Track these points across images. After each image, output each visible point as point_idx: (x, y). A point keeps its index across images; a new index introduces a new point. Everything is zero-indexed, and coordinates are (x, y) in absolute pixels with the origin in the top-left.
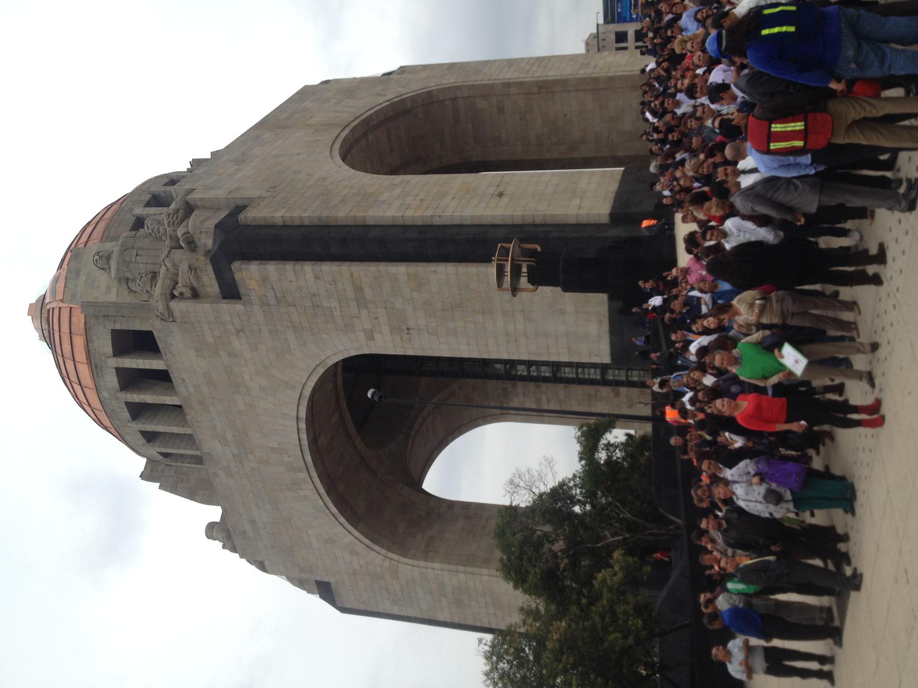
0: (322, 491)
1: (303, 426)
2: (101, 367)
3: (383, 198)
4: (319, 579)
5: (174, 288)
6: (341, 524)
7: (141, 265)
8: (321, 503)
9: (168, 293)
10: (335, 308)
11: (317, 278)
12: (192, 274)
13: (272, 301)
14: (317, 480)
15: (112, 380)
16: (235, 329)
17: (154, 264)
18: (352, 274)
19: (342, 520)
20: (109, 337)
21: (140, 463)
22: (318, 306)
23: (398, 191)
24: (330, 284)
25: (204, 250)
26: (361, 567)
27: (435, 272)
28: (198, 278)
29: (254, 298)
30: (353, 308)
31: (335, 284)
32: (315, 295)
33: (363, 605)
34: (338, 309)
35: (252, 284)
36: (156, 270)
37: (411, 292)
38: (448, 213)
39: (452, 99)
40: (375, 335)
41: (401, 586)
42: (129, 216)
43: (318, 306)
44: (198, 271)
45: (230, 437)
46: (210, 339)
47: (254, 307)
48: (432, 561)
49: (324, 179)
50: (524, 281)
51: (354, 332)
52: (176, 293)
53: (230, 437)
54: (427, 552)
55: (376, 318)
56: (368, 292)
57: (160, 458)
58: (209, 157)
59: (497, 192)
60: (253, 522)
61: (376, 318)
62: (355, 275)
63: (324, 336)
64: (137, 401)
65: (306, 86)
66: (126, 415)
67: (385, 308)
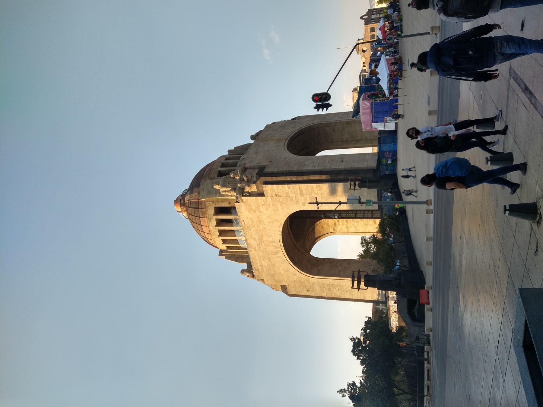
1: (281, 233)
2: (211, 219)
3: (306, 163)
4: (282, 284)
11: (289, 188)
14: (284, 251)
17: (234, 186)
18: (299, 187)
19: (291, 263)
22: (288, 196)
23: (310, 161)
29: (269, 195)
30: (299, 196)
32: (287, 193)
34: (295, 197)
35: (269, 191)
36: (235, 188)
38: (328, 168)
39: (317, 128)
40: (305, 204)
42: (216, 171)
43: (288, 196)
45: (257, 238)
46: (254, 208)
49: (285, 158)
50: (357, 187)
53: (257, 238)
56: (304, 192)
58: (234, 149)
59: (341, 161)
60: (262, 266)
62: (300, 187)
64: (222, 229)
65: (267, 125)
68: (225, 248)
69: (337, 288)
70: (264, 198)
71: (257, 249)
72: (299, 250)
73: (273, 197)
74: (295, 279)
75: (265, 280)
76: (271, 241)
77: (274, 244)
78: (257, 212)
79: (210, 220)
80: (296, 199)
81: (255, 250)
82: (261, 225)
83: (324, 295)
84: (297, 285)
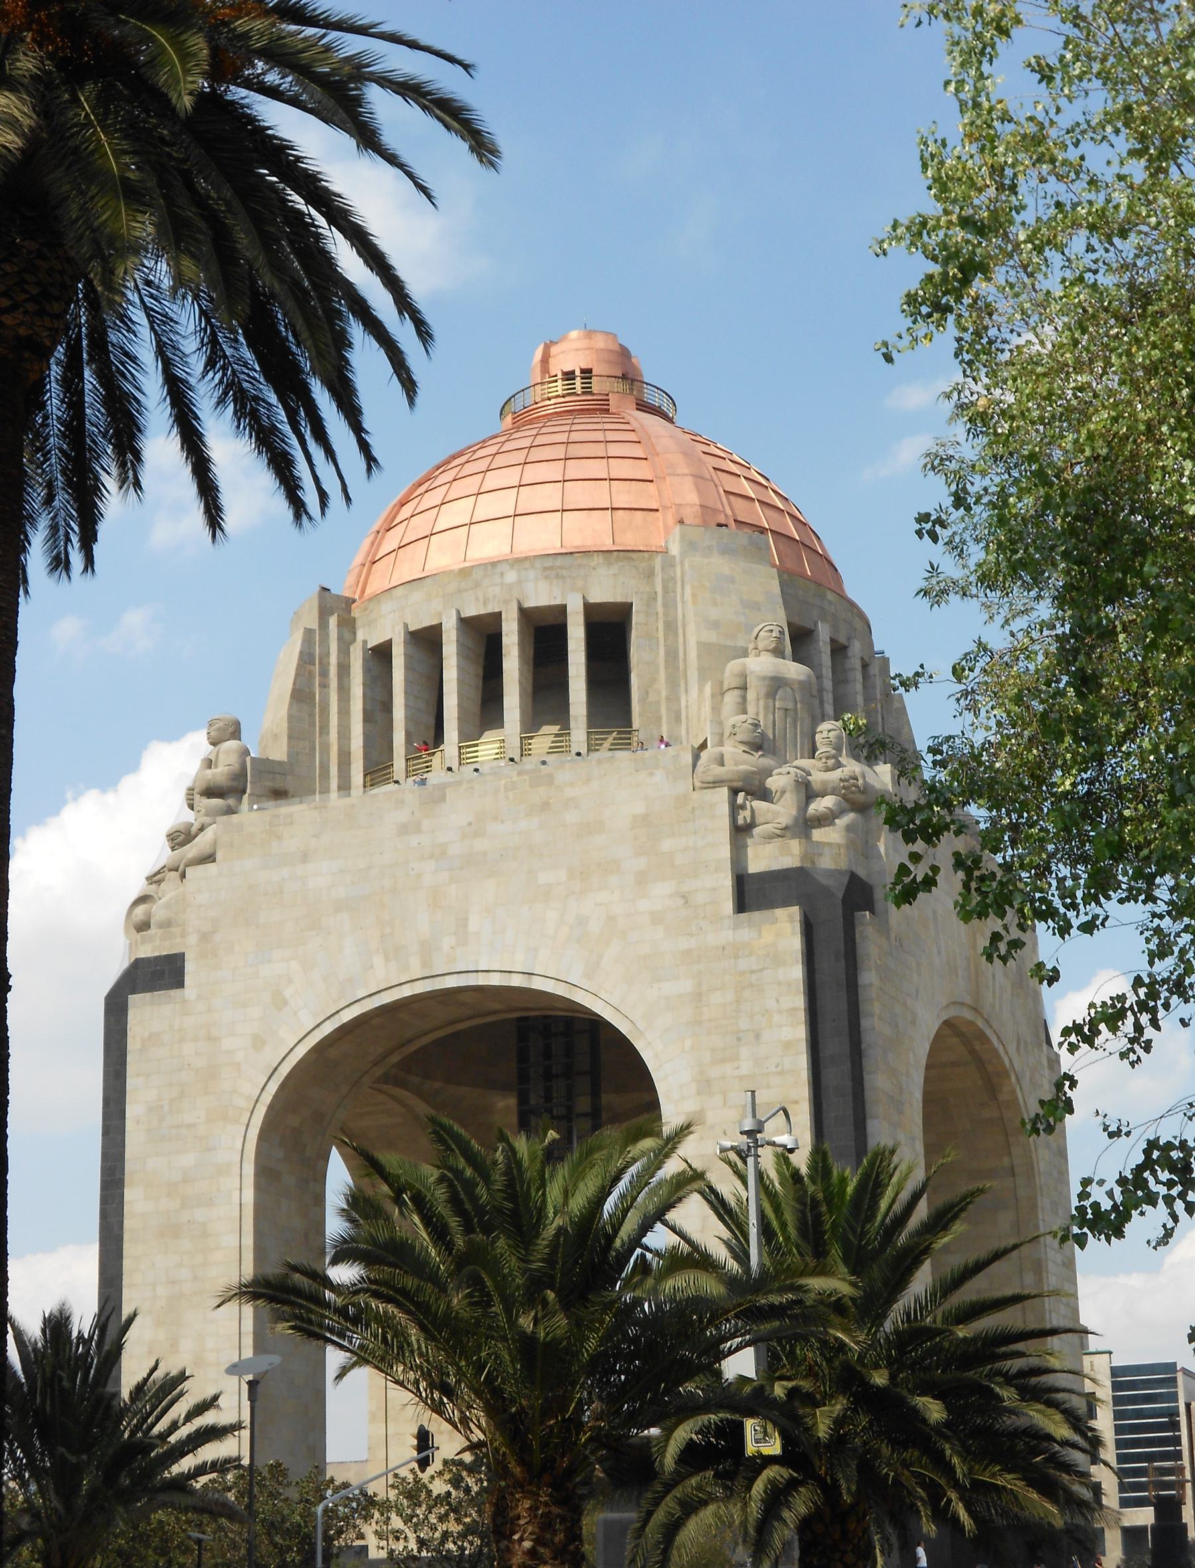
2: (563, 577)
5: (747, 793)
6: (318, 1025)
11: (788, 1045)
13: (743, 964)
14: (407, 992)
15: (541, 596)
22: (739, 1039)
29: (745, 934)
31: (779, 1073)
35: (768, 935)
39: (1012, 1169)
43: (739, 1039)
46: (667, 845)
47: (731, 932)
51: (699, 1093)
52: (741, 797)
63: (688, 1043)
68: (370, 635)
70: (728, 905)
71: (414, 840)
72: (375, 1065)
73: (736, 957)
74: (227, 1044)
76: (463, 922)
77: (447, 942)
81: (404, 830)
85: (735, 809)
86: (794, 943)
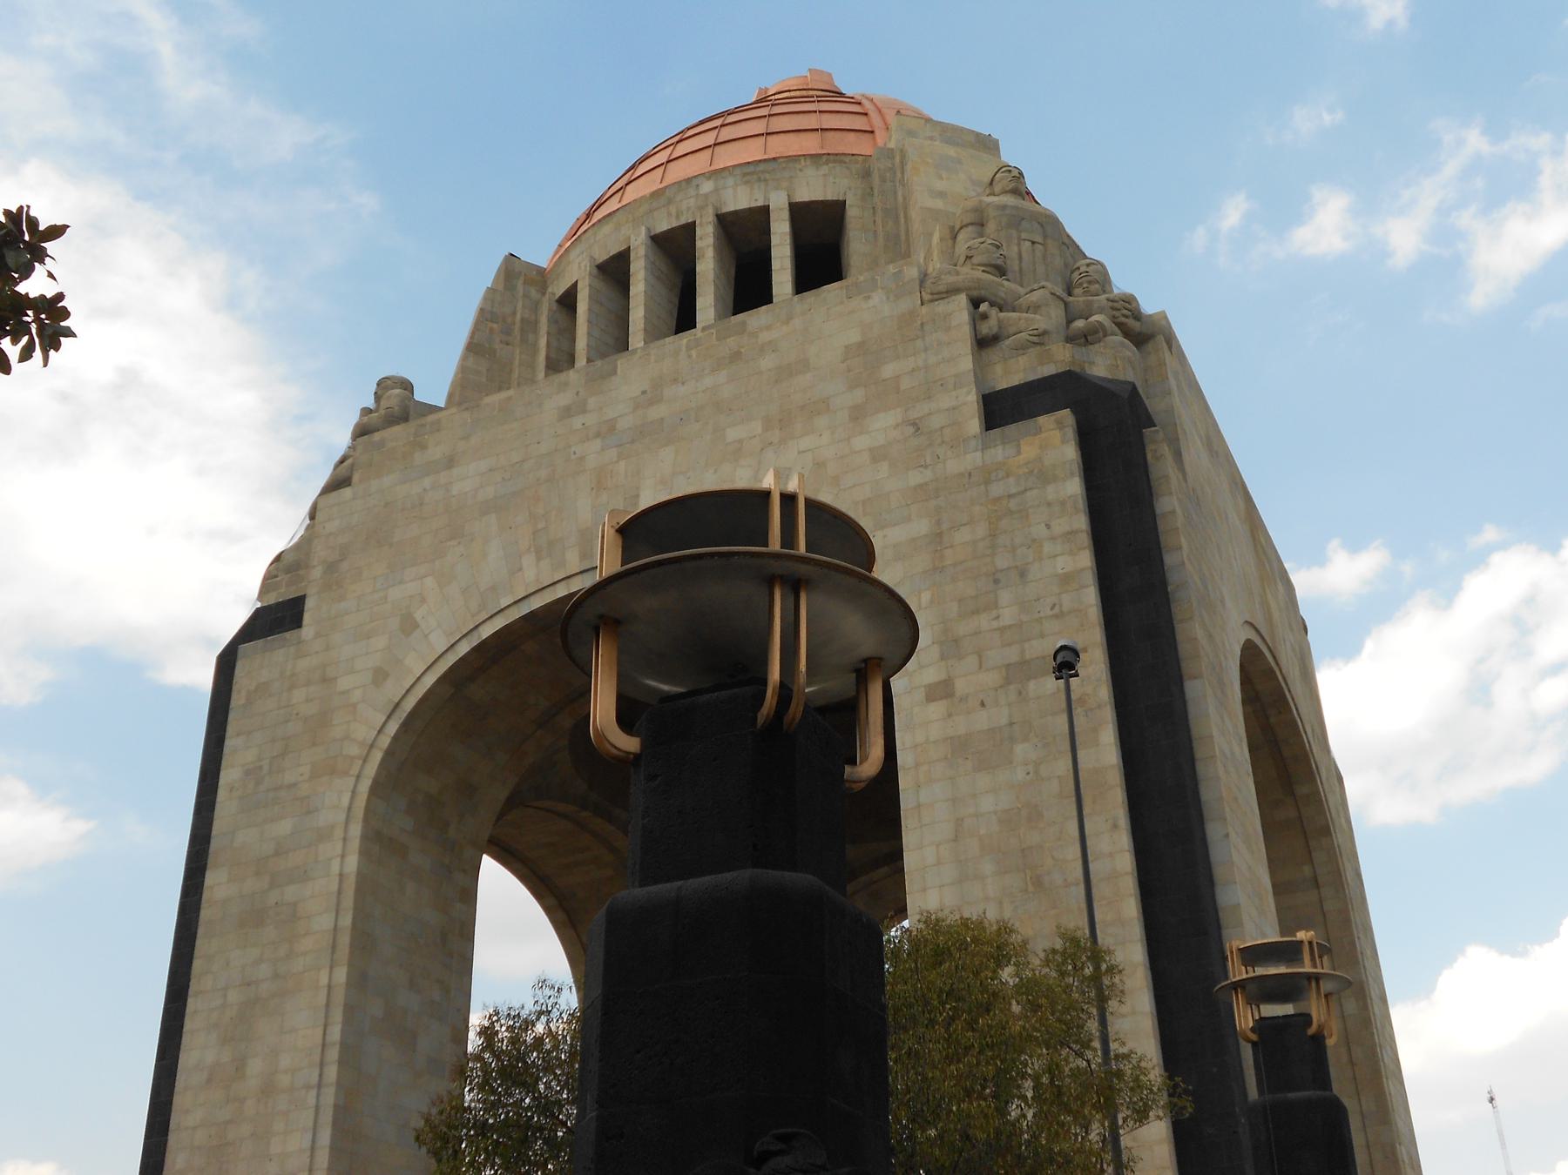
0: (536, 603)
4: (309, 604)
5: (992, 304)
7: (1015, 249)
8: (504, 602)
9: (983, 292)
10: (998, 617)
11: (1066, 579)
12: (1028, 337)
13: (997, 489)
15: (739, 199)
16: (921, 418)
19: (464, 648)
20: (830, 195)
21: (539, 255)
22: (996, 581)
24: (1054, 605)
25: (1084, 362)
26: (343, 693)
27: (1115, 826)
28: (1022, 348)
29: (998, 453)
31: (1056, 616)
33: (242, 701)
34: (995, 624)
35: (1029, 450)
37: (1059, 777)
41: (294, 785)
43: (996, 581)
44: (1038, 348)
45: (655, 413)
46: (888, 371)
47: (979, 454)
48: (364, 853)
51: (943, 657)
52: (984, 307)
53: (655, 413)
54: (378, 842)
55: (983, 704)
57: (560, 289)
60: (450, 462)
61: (983, 704)
66: (663, 225)
67: (1011, 724)
69: (264, 970)
71: (577, 422)
73: (987, 482)
74: (344, 683)
75: (347, 493)
78: (859, 395)
79: (759, 180)
80: (977, 633)
81: (567, 413)
82: (757, 427)
83: (216, 881)
84: (298, 695)
85: (978, 318)
86: (1070, 452)
